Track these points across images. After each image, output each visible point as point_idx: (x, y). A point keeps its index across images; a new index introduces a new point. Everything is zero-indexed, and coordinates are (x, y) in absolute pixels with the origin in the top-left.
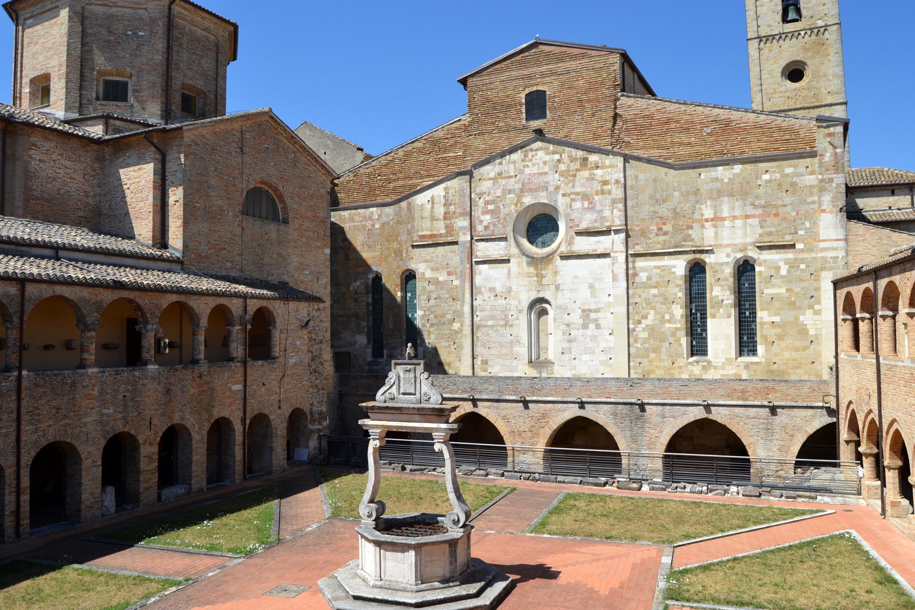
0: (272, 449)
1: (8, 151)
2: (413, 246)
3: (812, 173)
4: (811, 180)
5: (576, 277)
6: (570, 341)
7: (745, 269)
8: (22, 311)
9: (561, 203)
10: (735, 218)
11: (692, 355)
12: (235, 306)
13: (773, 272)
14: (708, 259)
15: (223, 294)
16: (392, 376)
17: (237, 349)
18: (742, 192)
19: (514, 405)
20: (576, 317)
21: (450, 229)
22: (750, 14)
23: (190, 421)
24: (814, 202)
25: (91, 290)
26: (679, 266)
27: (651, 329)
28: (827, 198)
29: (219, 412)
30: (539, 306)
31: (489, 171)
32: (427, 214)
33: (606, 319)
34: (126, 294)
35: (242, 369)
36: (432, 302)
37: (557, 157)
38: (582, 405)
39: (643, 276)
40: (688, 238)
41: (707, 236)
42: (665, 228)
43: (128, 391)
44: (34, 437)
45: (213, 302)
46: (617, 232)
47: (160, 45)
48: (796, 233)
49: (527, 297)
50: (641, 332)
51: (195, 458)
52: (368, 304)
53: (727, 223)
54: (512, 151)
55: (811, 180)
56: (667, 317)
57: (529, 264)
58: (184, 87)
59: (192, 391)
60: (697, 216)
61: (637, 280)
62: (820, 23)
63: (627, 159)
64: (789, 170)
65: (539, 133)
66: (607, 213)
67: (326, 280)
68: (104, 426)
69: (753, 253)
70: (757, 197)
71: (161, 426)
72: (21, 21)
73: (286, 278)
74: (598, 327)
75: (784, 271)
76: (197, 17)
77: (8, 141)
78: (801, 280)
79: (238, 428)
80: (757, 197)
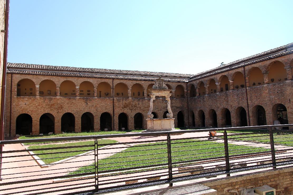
34: (273, 60)
43: (279, 90)
68: (272, 101)
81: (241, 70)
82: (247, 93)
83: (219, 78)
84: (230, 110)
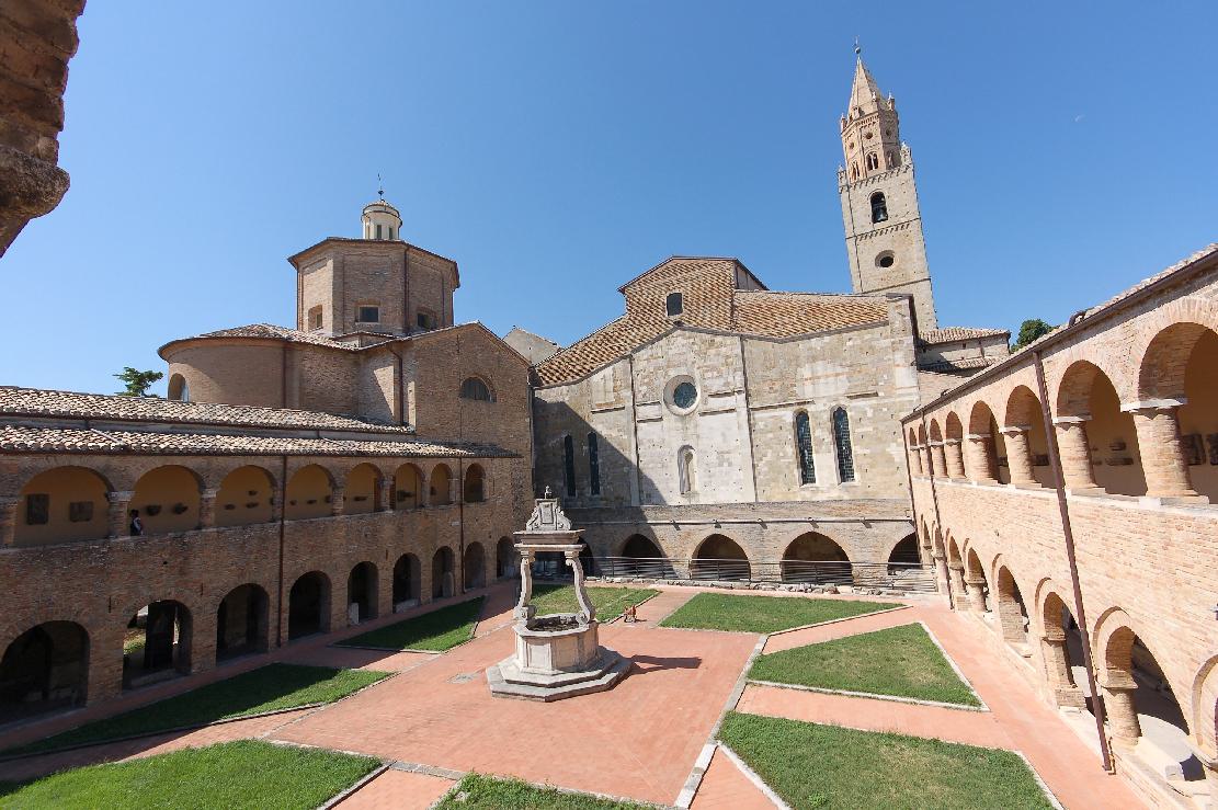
0: (485, 568)
1: (288, 363)
2: (594, 412)
3: (886, 337)
4: (886, 342)
5: (711, 428)
6: (710, 477)
7: (839, 416)
8: (285, 478)
9: (697, 375)
10: (827, 376)
11: (804, 483)
12: (453, 465)
13: (861, 415)
14: (810, 409)
15: (443, 456)
16: (536, 513)
17: (455, 496)
18: (833, 356)
19: (668, 527)
20: (713, 458)
21: (618, 399)
22: (847, 219)
23: (418, 551)
24: (889, 359)
25: (339, 459)
26: (788, 416)
27: (769, 463)
28: (899, 357)
29: (440, 544)
30: (686, 453)
31: (644, 354)
32: (601, 388)
33: (736, 458)
34: (365, 461)
35: (459, 511)
36: (609, 452)
37: (692, 340)
38: (718, 525)
39: (760, 425)
40: (793, 394)
41: (807, 392)
42: (777, 387)
44: (294, 569)
45: (433, 464)
46: (739, 392)
47: (399, 280)
48: (877, 384)
49: (679, 444)
50: (762, 467)
51: (423, 577)
52: (562, 456)
53: (822, 380)
54: (659, 338)
55: (886, 342)
56: (781, 454)
57: (676, 421)
58: (419, 309)
59: (420, 528)
60: (798, 377)
61: (757, 427)
62: (903, 220)
63: (742, 338)
64: (869, 336)
65: (679, 324)
66: (730, 379)
67: (529, 437)
69: (844, 402)
70: (845, 359)
71: (394, 558)
72: (301, 269)
73: (495, 441)
74: (730, 464)
75: (870, 414)
76: (427, 259)
77: (288, 355)
78: (886, 420)
79: (457, 554)
80: (845, 359)
81: (266, 463)
82: (282, 536)
83: (143, 472)
84: (191, 600)
